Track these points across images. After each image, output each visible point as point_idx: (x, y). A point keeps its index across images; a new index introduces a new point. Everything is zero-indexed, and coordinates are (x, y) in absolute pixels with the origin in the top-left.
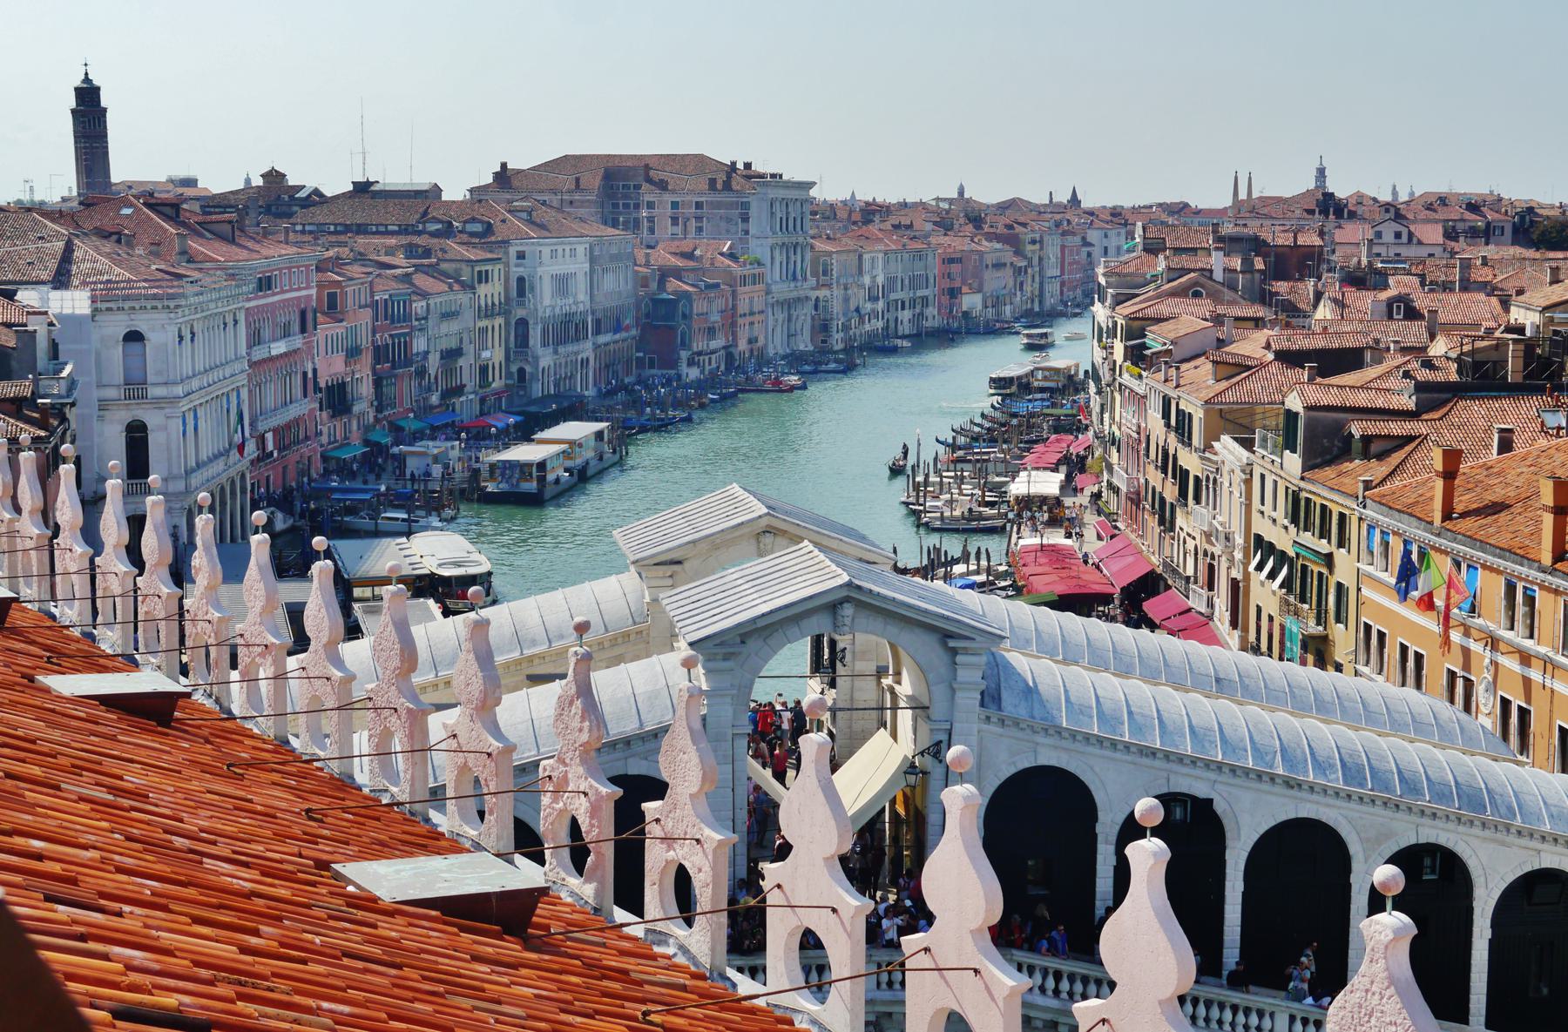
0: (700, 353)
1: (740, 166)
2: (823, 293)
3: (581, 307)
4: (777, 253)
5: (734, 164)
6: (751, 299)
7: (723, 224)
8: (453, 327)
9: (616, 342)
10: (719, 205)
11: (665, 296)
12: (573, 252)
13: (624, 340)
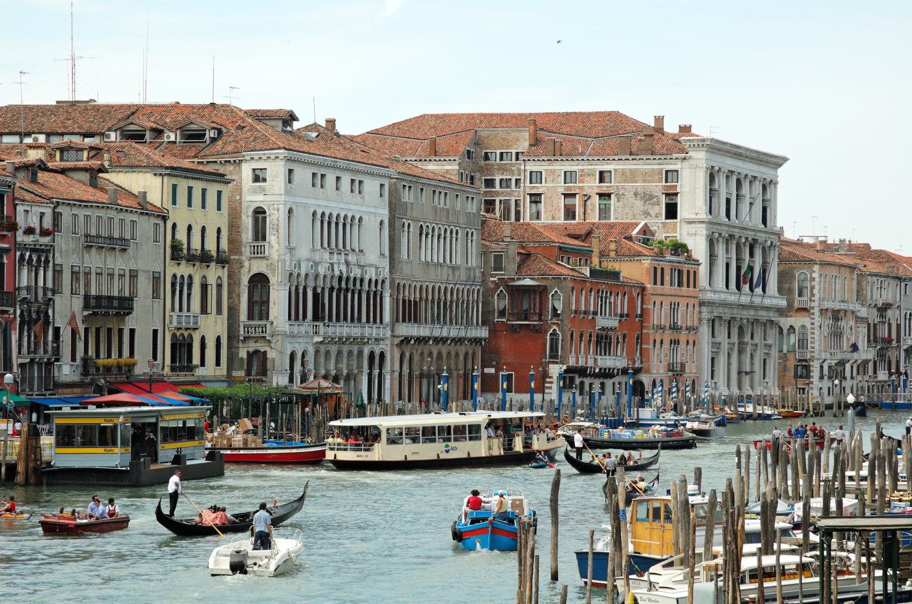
0: (582, 372)
1: (671, 128)
2: (797, 321)
3: (371, 274)
4: (720, 250)
5: (659, 120)
6: (674, 308)
7: (639, 204)
8: (118, 263)
9: (443, 340)
10: (632, 176)
11: (528, 282)
12: (357, 186)
13: (459, 341)
